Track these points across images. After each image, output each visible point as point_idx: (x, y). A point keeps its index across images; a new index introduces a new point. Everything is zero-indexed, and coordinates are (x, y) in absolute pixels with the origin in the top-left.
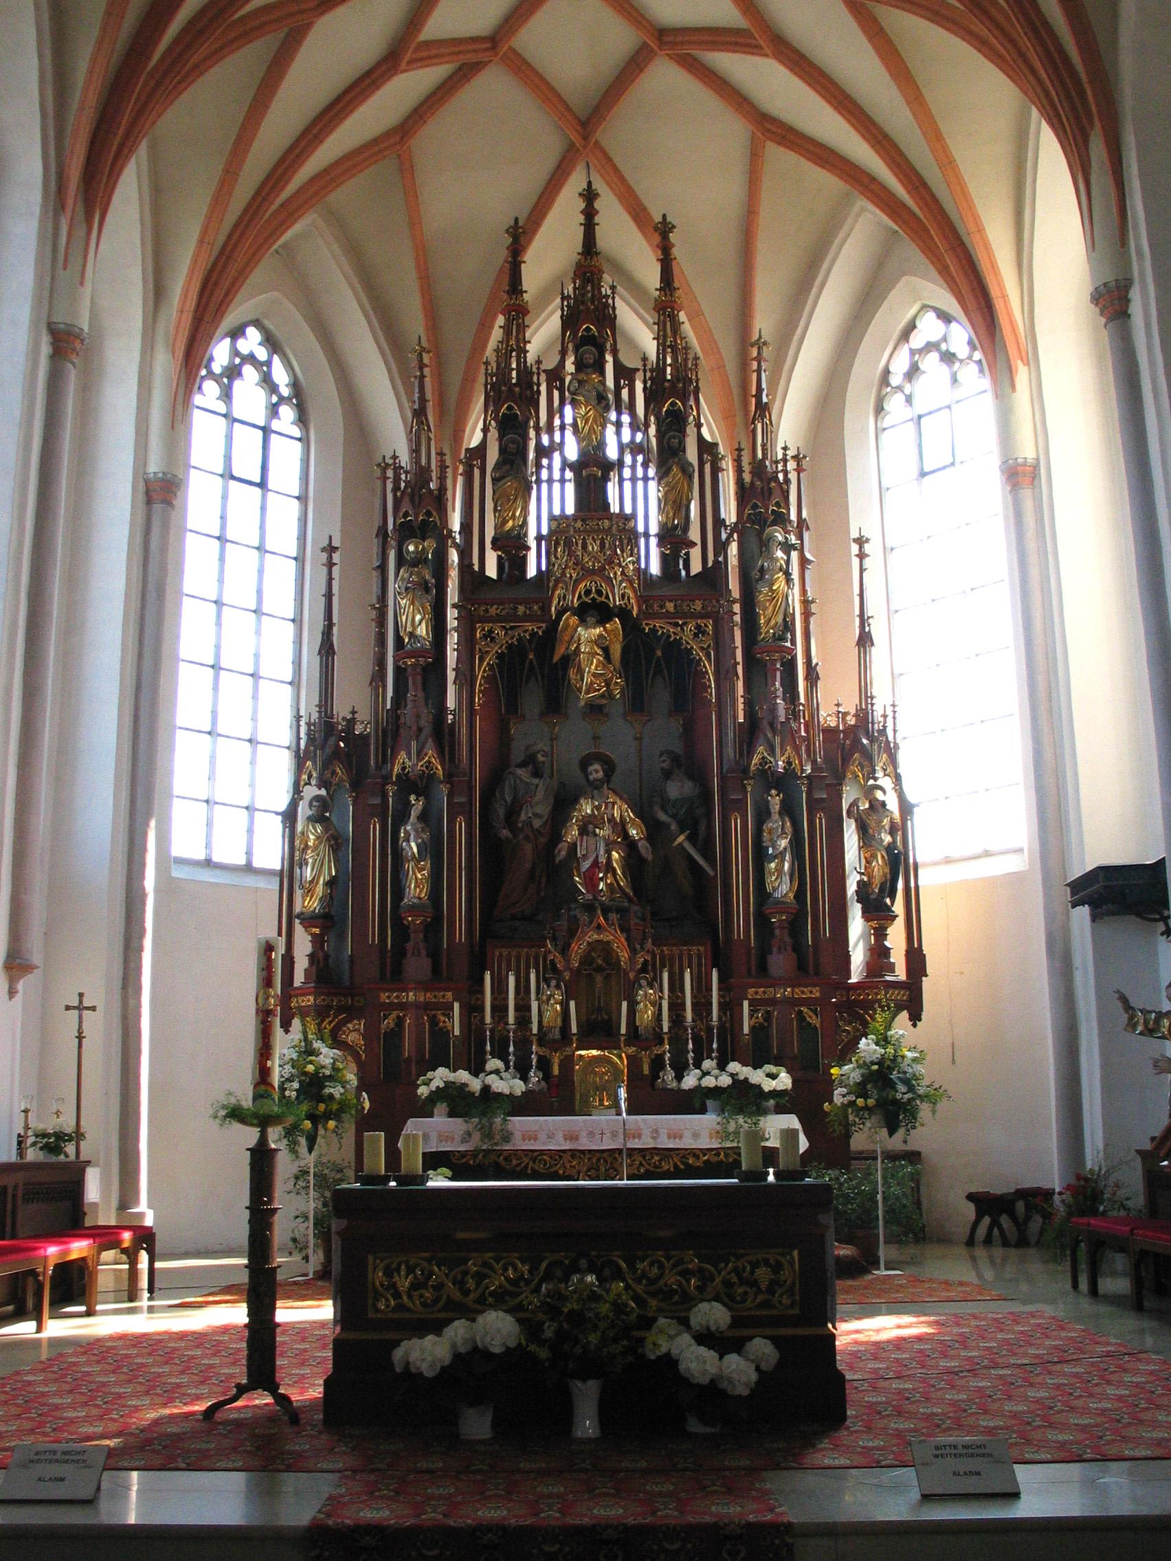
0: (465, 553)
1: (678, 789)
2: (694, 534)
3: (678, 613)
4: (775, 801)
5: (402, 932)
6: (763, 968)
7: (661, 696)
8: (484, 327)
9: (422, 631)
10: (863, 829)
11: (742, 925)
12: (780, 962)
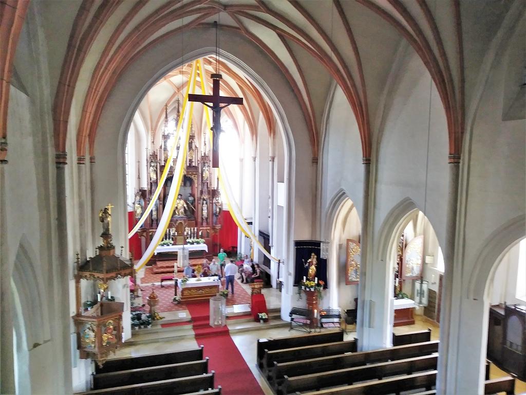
0: (160, 163)
1: (191, 199)
2: (194, 160)
3: (192, 174)
4: (205, 202)
5: (152, 221)
6: (202, 224)
7: (188, 183)
8: (160, 117)
9: (155, 177)
10: (216, 205)
11: (200, 220)
12: (204, 224)
